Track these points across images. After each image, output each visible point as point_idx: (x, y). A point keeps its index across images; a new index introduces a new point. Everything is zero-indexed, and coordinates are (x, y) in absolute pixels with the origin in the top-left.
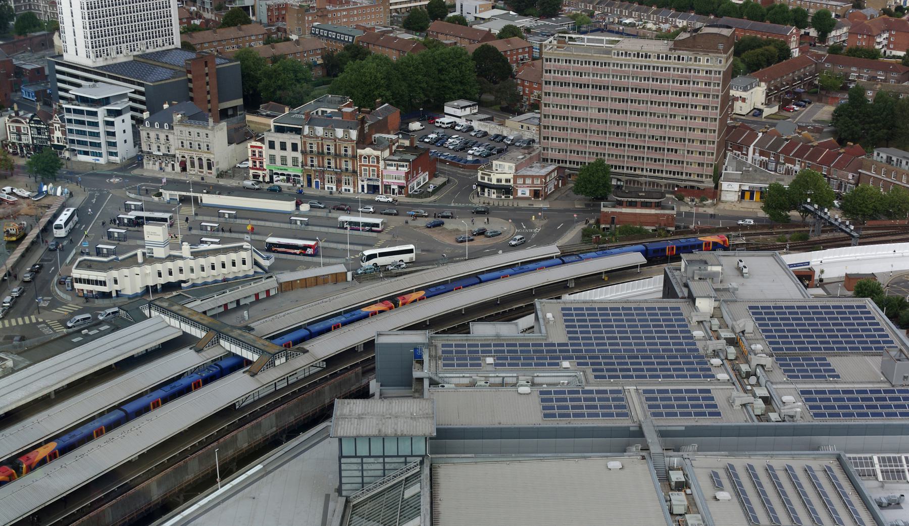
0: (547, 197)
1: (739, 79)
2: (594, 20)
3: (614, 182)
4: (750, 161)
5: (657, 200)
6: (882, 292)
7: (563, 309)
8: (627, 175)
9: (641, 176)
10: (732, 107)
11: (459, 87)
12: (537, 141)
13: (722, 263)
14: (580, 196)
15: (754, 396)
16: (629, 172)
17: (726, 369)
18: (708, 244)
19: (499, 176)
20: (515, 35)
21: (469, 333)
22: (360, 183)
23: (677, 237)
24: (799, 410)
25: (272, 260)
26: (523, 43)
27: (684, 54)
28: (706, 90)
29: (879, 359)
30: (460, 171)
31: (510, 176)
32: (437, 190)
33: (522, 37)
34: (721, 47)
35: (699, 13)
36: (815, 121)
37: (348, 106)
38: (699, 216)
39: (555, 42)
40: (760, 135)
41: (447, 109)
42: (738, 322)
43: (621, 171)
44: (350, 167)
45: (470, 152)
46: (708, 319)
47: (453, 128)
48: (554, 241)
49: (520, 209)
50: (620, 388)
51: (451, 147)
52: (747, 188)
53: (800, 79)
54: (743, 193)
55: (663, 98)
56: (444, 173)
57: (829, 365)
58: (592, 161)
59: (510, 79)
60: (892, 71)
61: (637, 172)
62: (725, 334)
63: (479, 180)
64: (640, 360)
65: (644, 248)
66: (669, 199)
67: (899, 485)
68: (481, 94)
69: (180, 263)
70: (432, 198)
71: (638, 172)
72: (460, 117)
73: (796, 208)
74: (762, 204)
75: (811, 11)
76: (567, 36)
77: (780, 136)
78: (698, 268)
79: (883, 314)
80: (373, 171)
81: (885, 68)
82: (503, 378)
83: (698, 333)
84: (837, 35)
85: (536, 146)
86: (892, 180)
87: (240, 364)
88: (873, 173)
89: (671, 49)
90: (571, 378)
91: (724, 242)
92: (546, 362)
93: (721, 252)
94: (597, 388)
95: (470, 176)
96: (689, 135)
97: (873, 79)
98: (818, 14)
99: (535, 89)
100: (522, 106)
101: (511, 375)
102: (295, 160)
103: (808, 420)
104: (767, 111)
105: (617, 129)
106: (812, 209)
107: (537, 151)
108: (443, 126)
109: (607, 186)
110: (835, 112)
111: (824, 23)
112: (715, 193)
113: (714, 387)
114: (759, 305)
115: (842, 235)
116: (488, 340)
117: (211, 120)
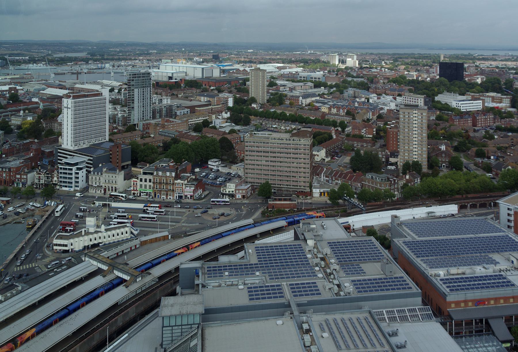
0: (248, 198)
1: (316, 147)
2: (262, 126)
3: (273, 191)
6: (377, 233)
7: (256, 248)
8: (277, 187)
9: (283, 188)
10: (314, 158)
14: (260, 197)
15: (334, 284)
16: (278, 186)
19: (229, 190)
21: (218, 261)
22: (175, 195)
23: (298, 213)
25: (138, 231)
26: (237, 135)
27: (295, 138)
29: (379, 264)
30: (214, 188)
31: (234, 190)
32: (205, 197)
33: (237, 133)
34: (308, 135)
35: (299, 123)
36: (344, 163)
37: (172, 163)
38: (306, 203)
39: (249, 135)
40: (325, 169)
41: (209, 163)
43: (275, 186)
44: (172, 188)
45: (218, 180)
46: (312, 249)
48: (251, 216)
49: (237, 204)
50: (280, 284)
52: (322, 191)
54: (321, 193)
55: (289, 156)
56: (208, 189)
57: (361, 268)
58: (264, 182)
62: (320, 256)
64: (287, 270)
66: (293, 197)
67: (395, 324)
68: (222, 156)
69: (100, 234)
70: (203, 200)
71: (282, 186)
73: (341, 199)
74: (328, 198)
77: (332, 170)
78: (306, 226)
79: (378, 243)
80: (181, 189)
81: (366, 142)
82: (232, 281)
83: (309, 256)
84: (348, 130)
86: (374, 186)
87: (121, 282)
88: (367, 183)
89: (290, 137)
92: (250, 273)
97: (362, 146)
102: (150, 186)
103: (355, 294)
104: (327, 160)
107: (243, 179)
109: (270, 192)
110: (351, 159)
111: (343, 126)
112: (311, 194)
114: (332, 241)
115: (359, 209)
117: (118, 170)
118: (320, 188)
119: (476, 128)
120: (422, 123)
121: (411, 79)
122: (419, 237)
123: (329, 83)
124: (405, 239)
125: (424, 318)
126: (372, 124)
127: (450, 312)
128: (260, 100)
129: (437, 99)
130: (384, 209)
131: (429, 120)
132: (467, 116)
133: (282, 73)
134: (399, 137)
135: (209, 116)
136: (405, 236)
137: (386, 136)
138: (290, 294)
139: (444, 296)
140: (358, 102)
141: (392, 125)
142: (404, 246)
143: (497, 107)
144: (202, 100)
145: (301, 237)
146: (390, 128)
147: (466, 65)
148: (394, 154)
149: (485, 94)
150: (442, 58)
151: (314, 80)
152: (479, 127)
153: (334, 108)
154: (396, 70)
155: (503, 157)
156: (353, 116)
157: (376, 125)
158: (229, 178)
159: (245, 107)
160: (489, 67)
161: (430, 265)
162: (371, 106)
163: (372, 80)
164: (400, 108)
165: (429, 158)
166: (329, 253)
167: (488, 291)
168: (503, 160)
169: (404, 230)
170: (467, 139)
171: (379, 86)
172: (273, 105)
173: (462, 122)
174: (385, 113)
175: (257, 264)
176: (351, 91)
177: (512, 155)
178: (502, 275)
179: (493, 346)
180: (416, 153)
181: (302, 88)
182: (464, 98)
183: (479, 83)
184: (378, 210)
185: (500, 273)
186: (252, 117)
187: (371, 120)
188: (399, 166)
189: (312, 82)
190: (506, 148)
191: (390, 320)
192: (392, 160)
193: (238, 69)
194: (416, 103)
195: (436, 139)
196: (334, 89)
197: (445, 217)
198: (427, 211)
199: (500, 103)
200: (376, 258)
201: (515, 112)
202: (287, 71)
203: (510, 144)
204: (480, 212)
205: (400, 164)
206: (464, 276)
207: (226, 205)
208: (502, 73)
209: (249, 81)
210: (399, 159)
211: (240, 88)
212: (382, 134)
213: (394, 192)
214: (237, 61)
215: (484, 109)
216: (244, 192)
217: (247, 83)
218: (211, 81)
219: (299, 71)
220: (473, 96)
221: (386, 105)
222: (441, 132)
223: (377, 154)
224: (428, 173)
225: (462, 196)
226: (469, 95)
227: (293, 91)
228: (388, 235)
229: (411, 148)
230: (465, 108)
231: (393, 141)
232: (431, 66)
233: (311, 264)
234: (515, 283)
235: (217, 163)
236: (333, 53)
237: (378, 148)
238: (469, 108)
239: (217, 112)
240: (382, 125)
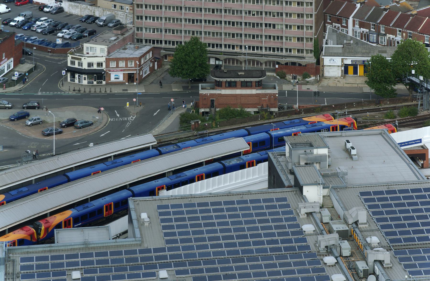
0: (142, 81)
3: (212, 62)
4: (350, 34)
8: (225, 53)
9: (240, 54)
14: (177, 79)
16: (227, 50)
17: (341, 269)
19: (90, 60)
21: (53, 242)
23: (281, 119)
30: (48, 56)
31: (102, 60)
38: (302, 94)
40: (358, 6)
42: (350, 211)
43: (219, 49)
45: (60, 35)
46: (317, 210)
51: (39, 31)
54: (346, 67)
58: (188, 40)
62: (338, 226)
66: (269, 77)
70: (18, 87)
71: (237, 50)
73: (401, 81)
74: (366, 79)
77: (378, 6)
83: (308, 228)
95: (59, 61)
106: (417, 81)
107: (131, 32)
109: (204, 66)
114: (371, 190)
118: (343, 54)
145: (288, 179)
216: (131, 65)
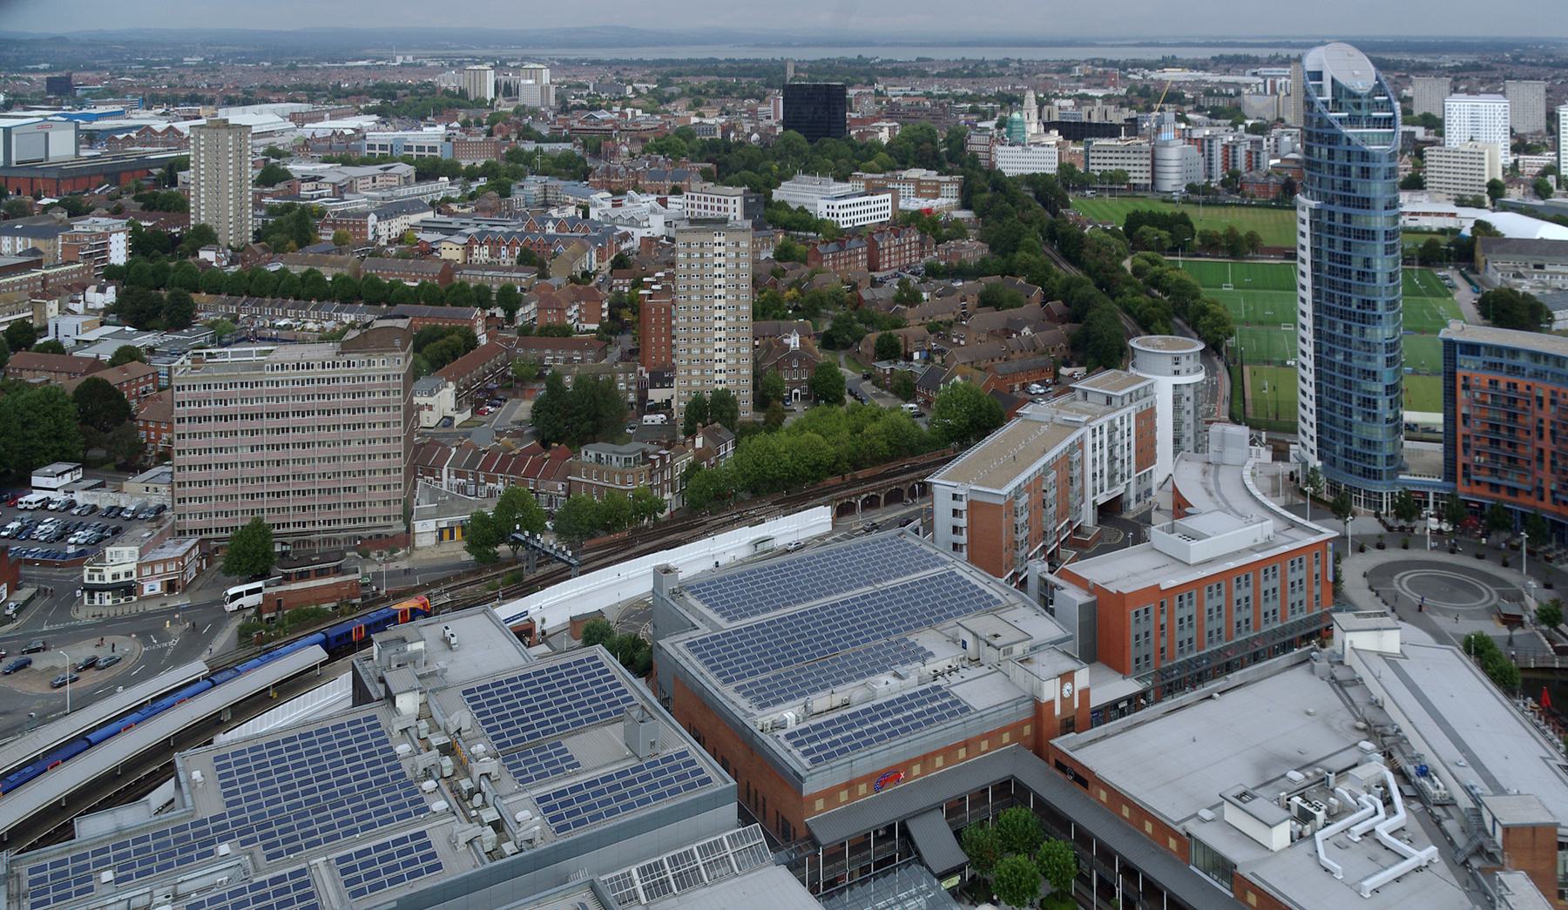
0: (186, 588)
1: (423, 382)
2: (238, 326)
4: (445, 488)
5: (335, 564)
6: (612, 633)
7: (216, 759)
8: (294, 534)
9: (313, 532)
11: (55, 444)
12: (169, 507)
13: (426, 636)
15: (482, 824)
16: (297, 529)
17: (443, 794)
18: (404, 612)
19: (115, 570)
20: (134, 360)
23: (366, 611)
24: (537, 828)
26: (145, 369)
27: (354, 357)
28: (385, 401)
29: (620, 725)
30: (56, 572)
31: (132, 567)
32: (20, 609)
33: (143, 361)
34: (397, 343)
35: (369, 302)
36: (513, 423)
38: (391, 574)
39: (189, 363)
40: (454, 450)
43: (286, 530)
45: (72, 540)
46: (414, 723)
47: (44, 507)
48: (200, 652)
49: (147, 615)
50: (304, 865)
51: (42, 538)
53: (492, 372)
54: (441, 531)
55: (333, 419)
56: (30, 581)
58: (247, 523)
59: (128, 421)
60: (587, 348)
61: (307, 528)
62: (438, 740)
63: (86, 581)
65: (323, 637)
67: (666, 902)
68: (86, 450)
71: (309, 528)
72: (55, 490)
73: (504, 541)
75: (494, 286)
76: (204, 351)
77: (476, 448)
78: (394, 650)
79: (617, 663)
81: (580, 346)
83: (402, 749)
84: (526, 312)
85: (167, 514)
86: (605, 483)
88: (584, 479)
89: (338, 354)
90: (233, 870)
91: (424, 605)
93: (420, 621)
94: (270, 876)
95: (72, 577)
96: (370, 464)
97: (569, 360)
98: (502, 289)
99: (165, 431)
100: (146, 459)
101: (141, 892)
104: (459, 419)
105: (277, 471)
106: (523, 538)
107: (170, 522)
108: (30, 507)
109: (268, 556)
110: (534, 407)
111: (510, 300)
112: (407, 538)
113: (429, 826)
115: (560, 565)
116: (103, 841)
119: (877, 275)
120: (737, 271)
121: (707, 138)
122: (730, 620)
123: (465, 164)
124: (693, 633)
125: (743, 862)
126: (598, 286)
127: (811, 825)
128: (229, 236)
129: (777, 195)
130: (632, 551)
131: (756, 262)
132: (854, 242)
133: (309, 136)
134: (674, 322)
135: (32, 306)
136: (693, 625)
137: (638, 322)
138: (339, 892)
139: (795, 781)
140: (555, 221)
141: (654, 287)
142: (690, 657)
143: (929, 211)
144: (6, 249)
145: (377, 690)
146: (650, 297)
147: (852, 92)
148: (662, 377)
149: (898, 173)
150: (790, 73)
151: (415, 153)
152: (885, 270)
153: (481, 245)
154: (667, 112)
155: (941, 352)
156: (542, 265)
157: (610, 289)
158: (114, 526)
159: (172, 264)
160: (908, 96)
161: (759, 699)
162: (596, 230)
163: (598, 145)
164: (677, 231)
165: (757, 376)
166: (466, 725)
167: (906, 740)
168: (943, 361)
169: (689, 608)
170: (855, 308)
171: (618, 163)
172: (278, 249)
173: (842, 261)
174: (636, 249)
175: (222, 816)
176: (533, 186)
177: (962, 342)
178: (939, 688)
179: (920, 893)
180: (722, 366)
181: (378, 183)
182: (846, 187)
183: (885, 142)
184: (616, 557)
185: (935, 683)
186: (201, 298)
187: (595, 274)
188: (675, 412)
189: (407, 160)
190: (950, 324)
191: (651, 893)
192: (656, 395)
193: (148, 128)
194: (722, 214)
195: (775, 317)
196: (483, 181)
197: (799, 547)
198: (752, 538)
199: (936, 196)
200: (611, 709)
201: (969, 220)
202: (325, 127)
203: (959, 311)
204: (888, 517)
205: (679, 406)
206: (846, 712)
207: (104, 626)
208: (940, 111)
209: (187, 168)
210: (674, 391)
211: (155, 196)
212: (627, 317)
213: (662, 495)
214: (144, 100)
215: (898, 217)
216: (172, 568)
217: (182, 176)
218: (40, 174)
219: (365, 124)
220: (868, 181)
221: (638, 225)
222: (788, 294)
223: (612, 383)
224: (755, 422)
225: (843, 478)
226: (860, 179)
227: (346, 196)
228: (645, 632)
229: (709, 351)
230: (849, 218)
231: (659, 335)
232: (761, 98)
233: (409, 775)
234: (970, 702)
235: (67, 478)
236: (476, 64)
237: (616, 363)
238: (859, 216)
239: (63, 290)
240: (626, 290)
